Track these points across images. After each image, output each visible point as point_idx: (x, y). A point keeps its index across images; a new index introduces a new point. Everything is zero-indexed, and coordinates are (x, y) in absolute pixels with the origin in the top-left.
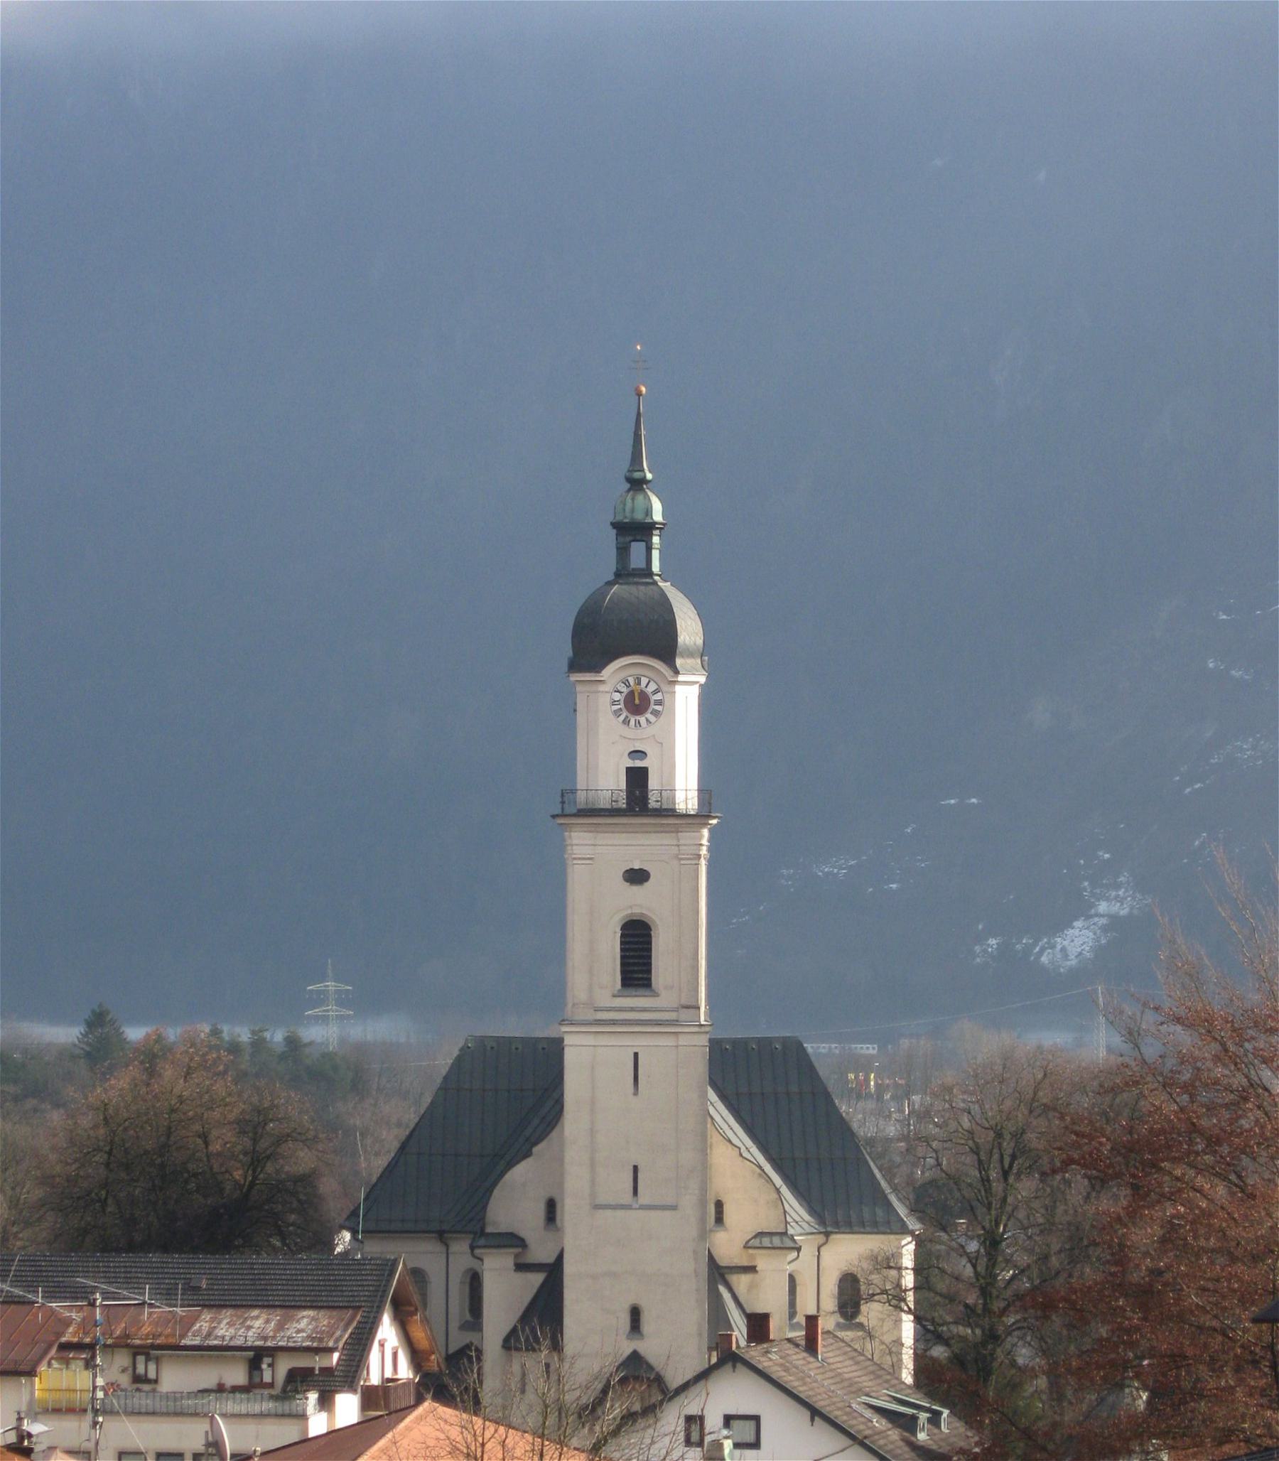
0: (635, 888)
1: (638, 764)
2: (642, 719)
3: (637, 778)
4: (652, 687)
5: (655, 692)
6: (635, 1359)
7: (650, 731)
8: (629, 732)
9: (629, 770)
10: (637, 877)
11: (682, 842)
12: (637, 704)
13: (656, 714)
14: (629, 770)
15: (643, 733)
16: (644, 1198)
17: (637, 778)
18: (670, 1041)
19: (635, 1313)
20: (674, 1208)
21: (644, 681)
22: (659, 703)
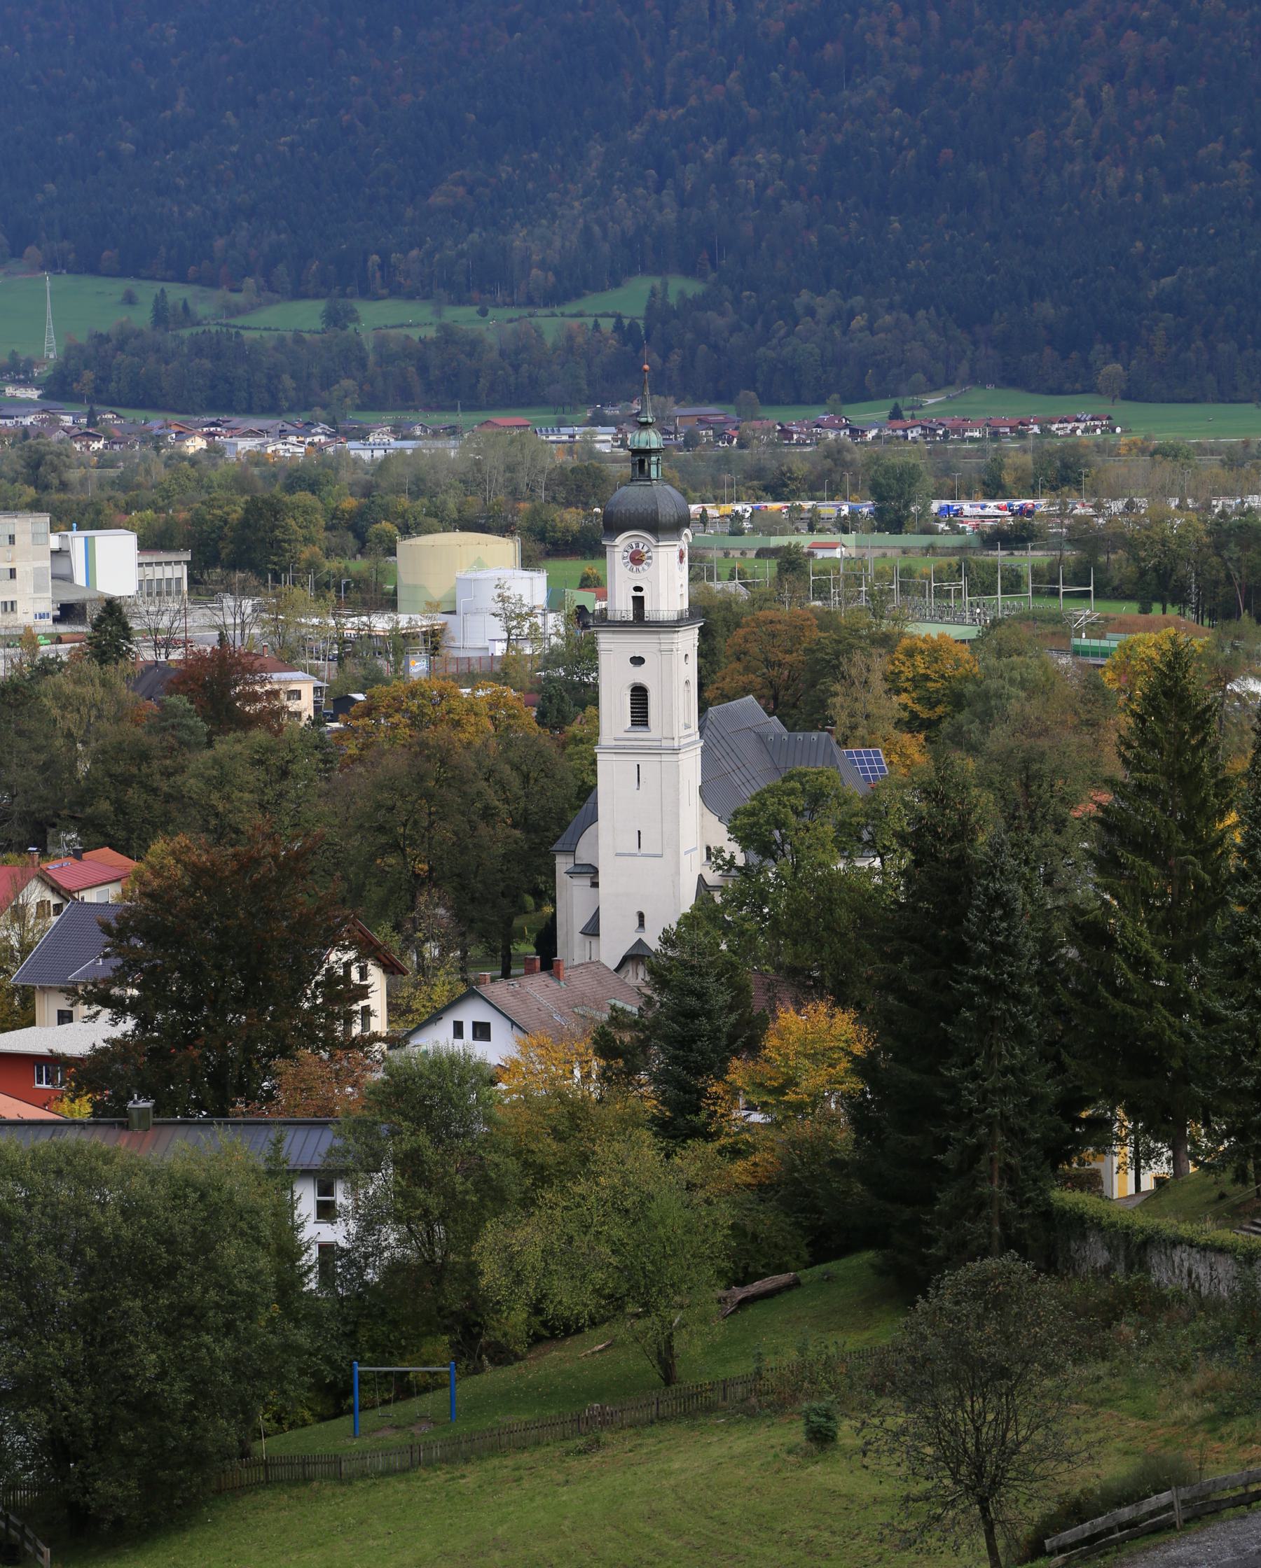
0: (637, 669)
1: (639, 594)
3: (639, 602)
4: (646, 549)
6: (640, 942)
7: (643, 575)
8: (632, 575)
9: (634, 598)
10: (638, 661)
12: (637, 559)
13: (649, 565)
14: (634, 598)
15: (641, 576)
16: (644, 850)
17: (639, 602)
18: (657, 758)
19: (641, 916)
20: (661, 856)
22: (650, 558)
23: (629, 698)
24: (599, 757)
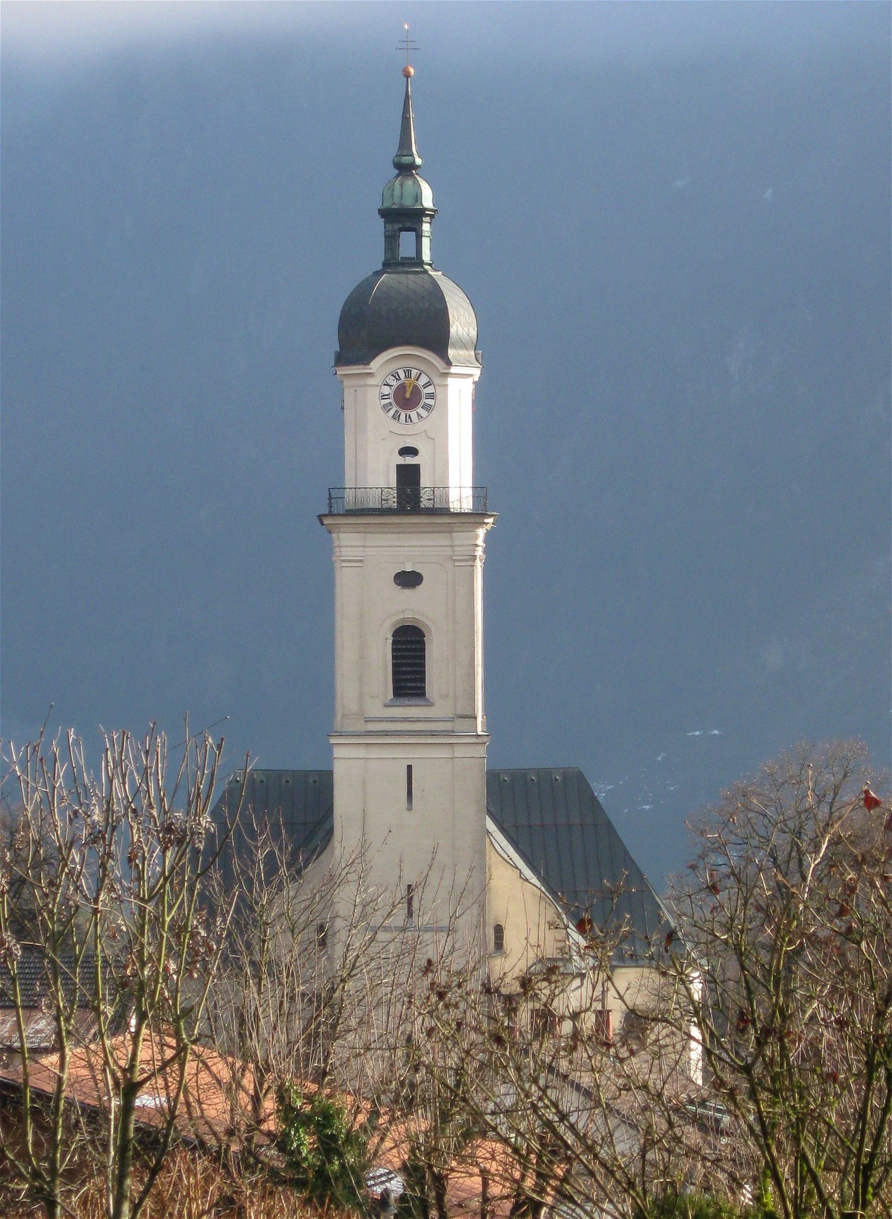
0: (408, 592)
1: (409, 460)
2: (413, 414)
3: (408, 476)
4: (423, 380)
5: (426, 386)
7: (419, 427)
8: (398, 427)
9: (400, 468)
10: (408, 580)
11: (456, 542)
12: (407, 398)
13: (428, 408)
14: (400, 468)
17: (408, 476)
21: (414, 372)
22: (431, 396)
23: (390, 641)
24: (338, 752)
